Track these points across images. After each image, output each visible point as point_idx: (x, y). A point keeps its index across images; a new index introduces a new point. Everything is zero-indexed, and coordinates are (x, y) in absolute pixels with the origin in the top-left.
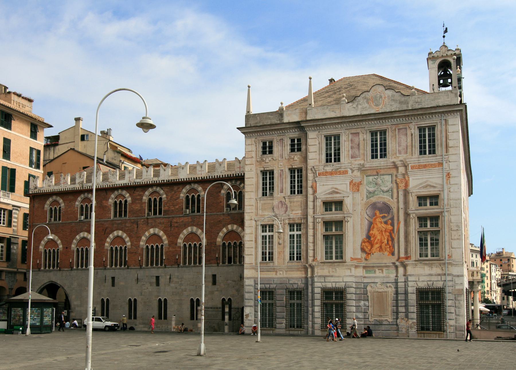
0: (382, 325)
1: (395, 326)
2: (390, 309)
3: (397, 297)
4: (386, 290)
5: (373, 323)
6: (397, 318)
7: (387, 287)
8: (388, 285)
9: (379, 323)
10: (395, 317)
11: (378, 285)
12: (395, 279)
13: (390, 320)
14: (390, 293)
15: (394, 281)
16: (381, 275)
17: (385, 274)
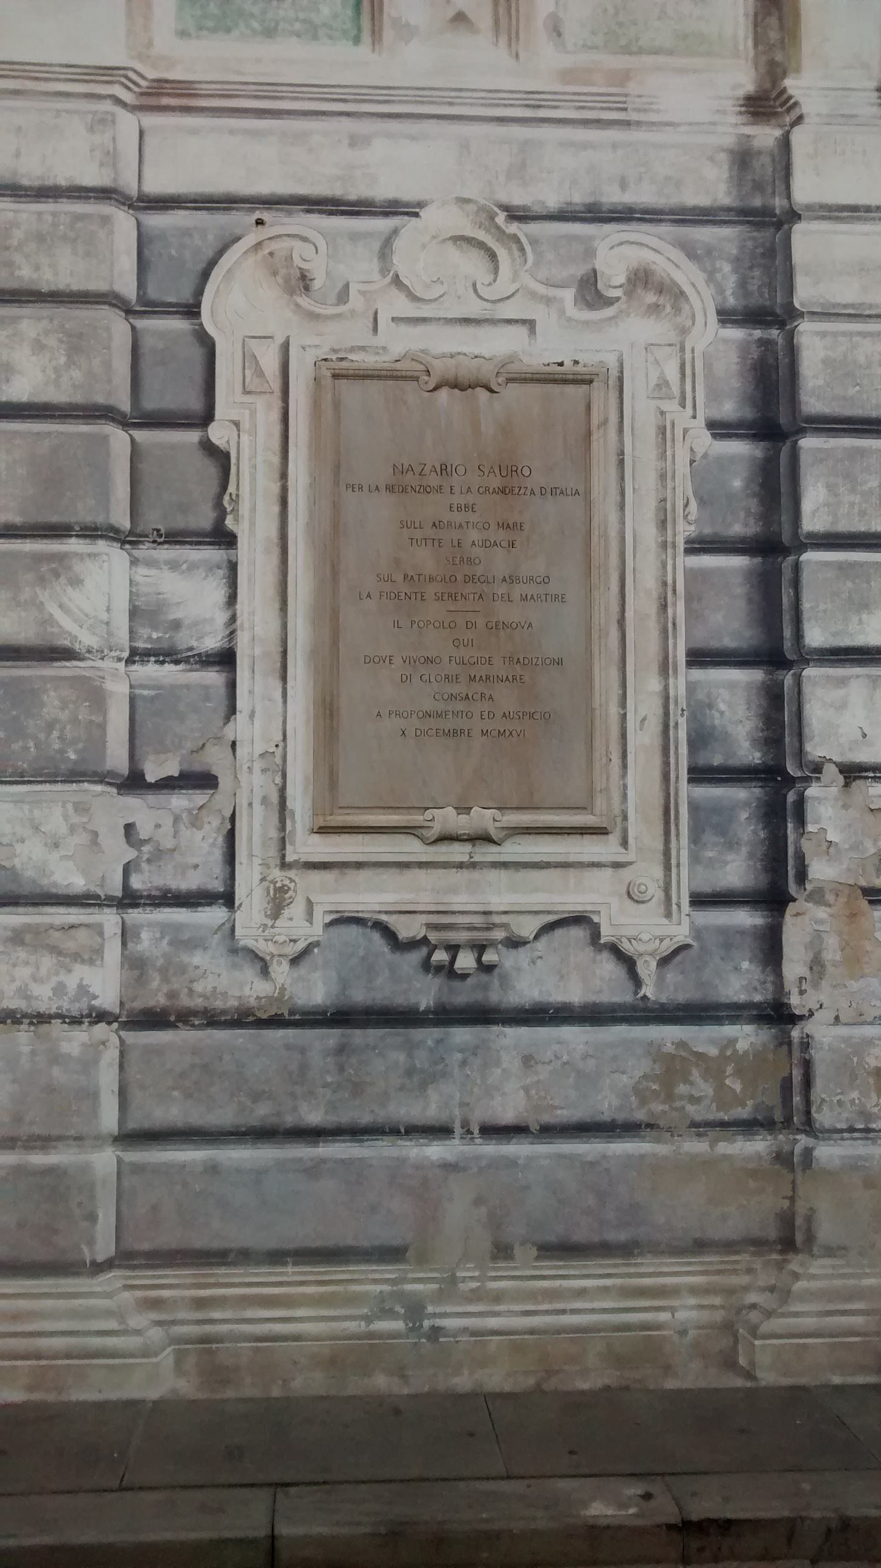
0: (483, 1016)
1: (746, 1036)
2: (644, 705)
3: (777, 486)
4: (560, 338)
5: (315, 990)
6: (773, 897)
7: (590, 291)
8: (616, 253)
9: (425, 993)
10: (736, 871)
11: (418, 250)
12: (743, 158)
13: (650, 927)
14: (641, 408)
15: (714, 186)
16: (482, 64)
17: (543, 65)
